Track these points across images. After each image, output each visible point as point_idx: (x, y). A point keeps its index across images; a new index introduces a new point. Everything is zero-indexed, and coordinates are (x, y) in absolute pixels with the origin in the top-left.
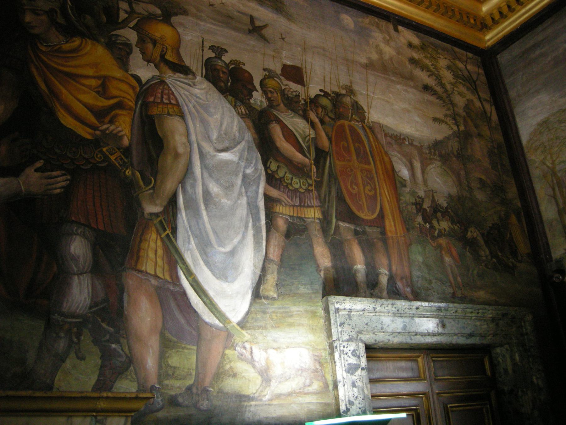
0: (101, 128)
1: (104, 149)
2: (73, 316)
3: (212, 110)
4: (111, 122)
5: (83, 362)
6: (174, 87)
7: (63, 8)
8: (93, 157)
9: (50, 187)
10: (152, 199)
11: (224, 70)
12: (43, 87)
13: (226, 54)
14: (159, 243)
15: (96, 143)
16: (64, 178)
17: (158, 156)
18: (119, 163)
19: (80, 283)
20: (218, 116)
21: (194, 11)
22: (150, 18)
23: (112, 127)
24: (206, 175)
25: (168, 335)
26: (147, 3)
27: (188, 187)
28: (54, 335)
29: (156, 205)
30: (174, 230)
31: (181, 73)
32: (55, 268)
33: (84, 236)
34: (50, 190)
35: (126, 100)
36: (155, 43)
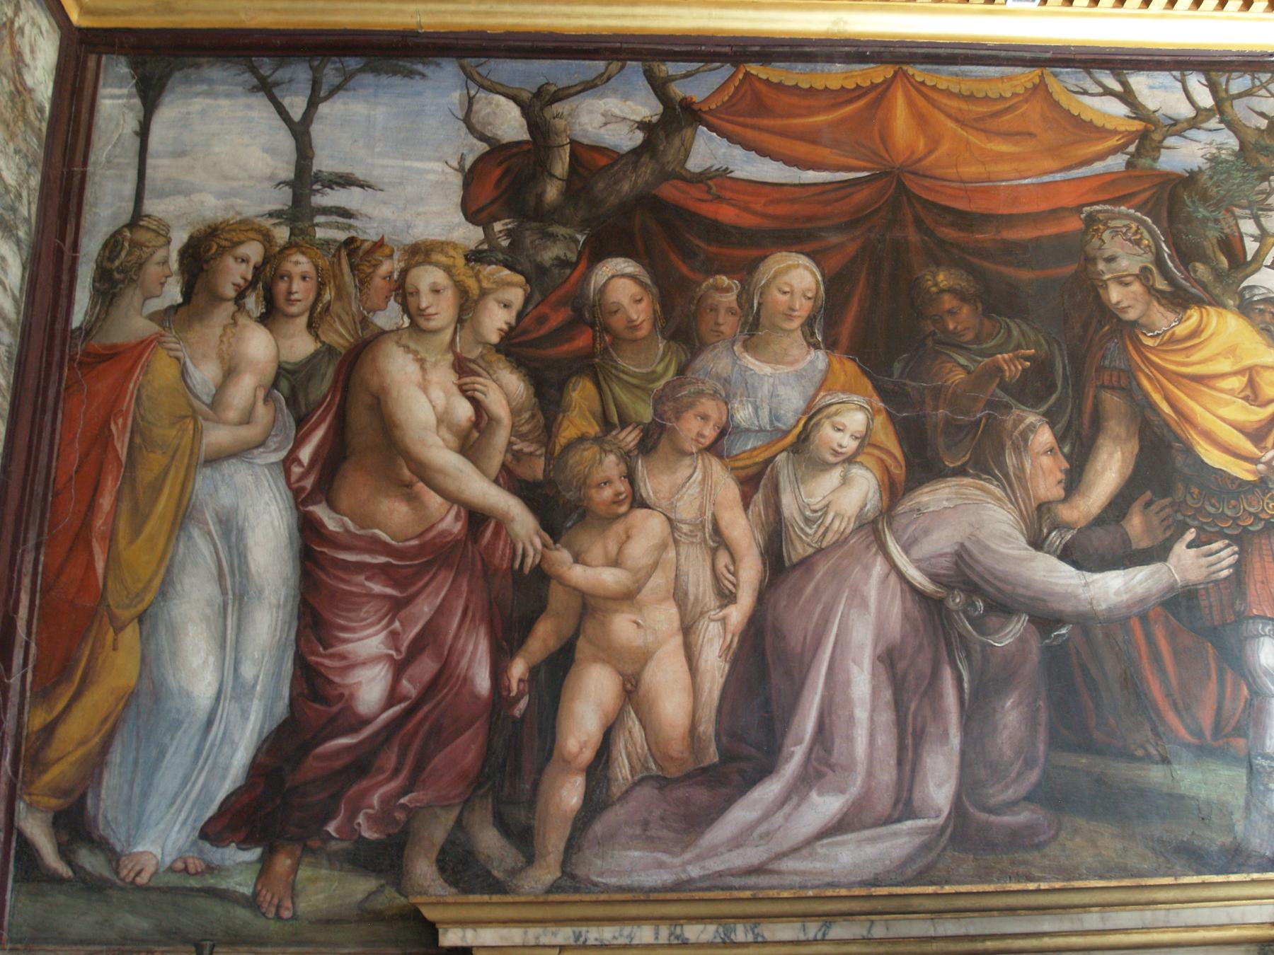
0: (1264, 459)
8: (1263, 509)
16: (1229, 550)
28: (1262, 788)
32: (1245, 691)
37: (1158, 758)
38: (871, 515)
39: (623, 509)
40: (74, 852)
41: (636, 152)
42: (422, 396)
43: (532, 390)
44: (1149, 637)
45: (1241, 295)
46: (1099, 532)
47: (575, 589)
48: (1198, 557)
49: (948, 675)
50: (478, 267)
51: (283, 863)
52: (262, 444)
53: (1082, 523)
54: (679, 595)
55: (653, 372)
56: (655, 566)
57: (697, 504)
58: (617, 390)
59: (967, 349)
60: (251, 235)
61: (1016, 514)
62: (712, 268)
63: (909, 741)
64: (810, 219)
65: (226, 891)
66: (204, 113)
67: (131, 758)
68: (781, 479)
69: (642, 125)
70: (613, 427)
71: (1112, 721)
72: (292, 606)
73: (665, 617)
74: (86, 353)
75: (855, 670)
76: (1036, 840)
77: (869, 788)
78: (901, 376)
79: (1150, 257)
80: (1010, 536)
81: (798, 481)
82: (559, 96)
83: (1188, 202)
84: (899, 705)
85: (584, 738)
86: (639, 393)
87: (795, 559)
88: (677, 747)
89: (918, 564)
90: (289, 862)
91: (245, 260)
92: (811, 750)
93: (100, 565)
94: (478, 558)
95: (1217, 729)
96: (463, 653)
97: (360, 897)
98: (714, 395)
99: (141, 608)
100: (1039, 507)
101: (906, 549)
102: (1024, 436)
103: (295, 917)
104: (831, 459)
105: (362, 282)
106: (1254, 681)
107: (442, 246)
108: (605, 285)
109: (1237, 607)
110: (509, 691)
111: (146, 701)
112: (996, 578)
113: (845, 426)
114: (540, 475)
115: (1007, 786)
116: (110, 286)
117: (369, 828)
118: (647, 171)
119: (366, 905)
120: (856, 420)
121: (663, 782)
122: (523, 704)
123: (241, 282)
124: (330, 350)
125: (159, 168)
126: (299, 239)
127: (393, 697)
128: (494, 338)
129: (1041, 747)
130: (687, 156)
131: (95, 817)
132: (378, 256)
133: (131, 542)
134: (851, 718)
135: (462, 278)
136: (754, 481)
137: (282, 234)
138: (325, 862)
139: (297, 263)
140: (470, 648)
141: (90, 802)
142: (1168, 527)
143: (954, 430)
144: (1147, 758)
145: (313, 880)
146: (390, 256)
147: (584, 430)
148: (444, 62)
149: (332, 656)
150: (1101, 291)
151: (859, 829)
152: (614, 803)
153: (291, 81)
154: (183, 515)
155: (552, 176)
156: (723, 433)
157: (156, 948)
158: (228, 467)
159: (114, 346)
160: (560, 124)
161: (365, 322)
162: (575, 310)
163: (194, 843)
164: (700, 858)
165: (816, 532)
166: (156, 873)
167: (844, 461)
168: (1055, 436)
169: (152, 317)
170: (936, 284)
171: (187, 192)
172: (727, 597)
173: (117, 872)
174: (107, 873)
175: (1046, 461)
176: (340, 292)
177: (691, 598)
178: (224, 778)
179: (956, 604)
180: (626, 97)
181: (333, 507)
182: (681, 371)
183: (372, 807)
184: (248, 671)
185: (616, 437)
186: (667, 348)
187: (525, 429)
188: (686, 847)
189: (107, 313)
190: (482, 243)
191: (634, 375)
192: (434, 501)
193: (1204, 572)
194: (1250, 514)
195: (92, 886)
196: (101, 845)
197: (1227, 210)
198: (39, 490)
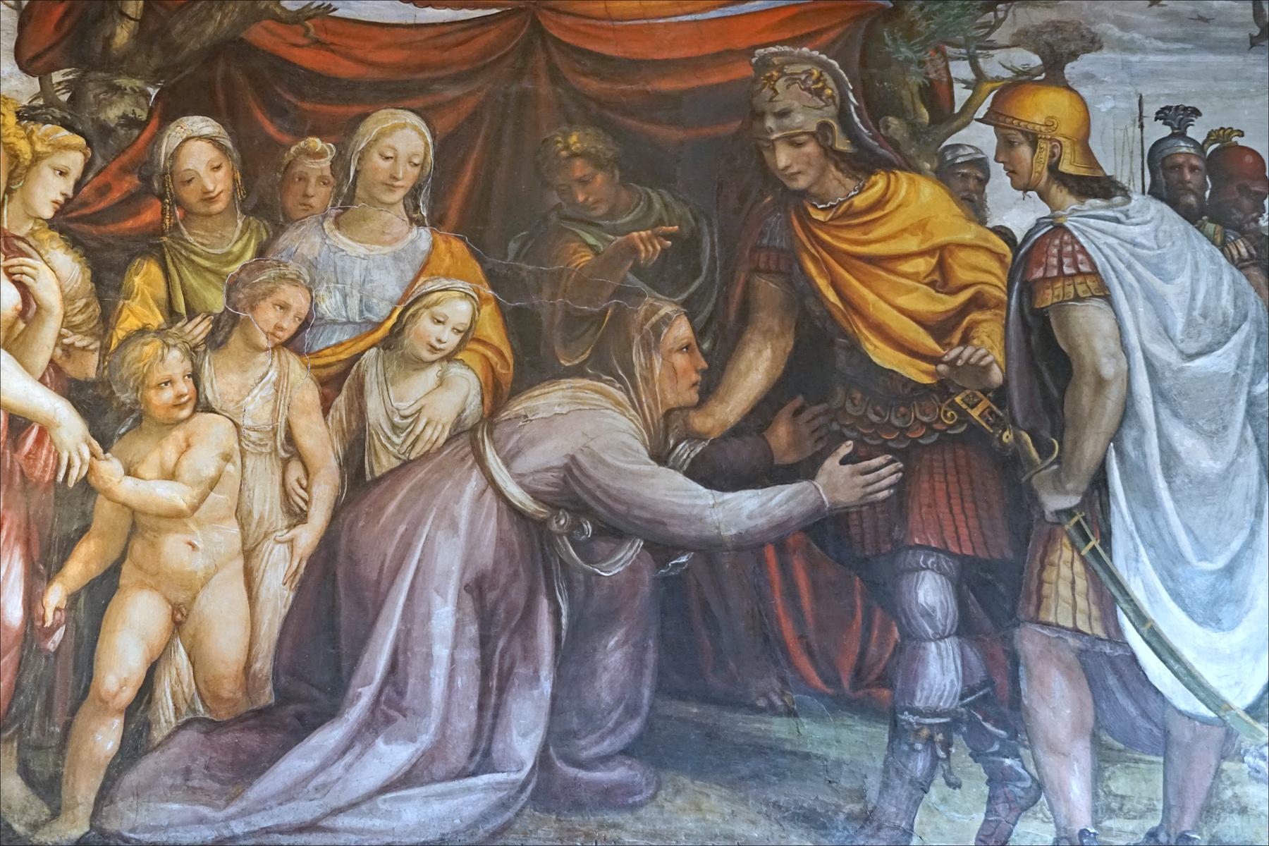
0: (946, 358)
1: (958, 399)
2: (935, 714)
3: (1171, 267)
4: (965, 341)
5: (958, 791)
6: (1083, 233)
7: (843, 115)
8: (939, 418)
9: (870, 489)
10: (1058, 484)
11: (1195, 162)
12: (831, 296)
13: (1197, 121)
14: (1078, 567)
15: (943, 389)
16: (892, 467)
17: (1063, 392)
18: (987, 422)
19: (940, 654)
20: (1185, 279)
21: (1116, 32)
22: (1020, 82)
23: (968, 352)
24: (1165, 413)
25: (1106, 738)
26: (1008, 47)
27: (1129, 446)
28: (906, 748)
29: (1067, 493)
30: (1106, 539)
31: (1096, 196)
32: (896, 634)
33: (939, 570)
34: (871, 494)
35: (987, 288)
36: (1033, 140)
37: (782, 709)
38: (469, 423)
39: (186, 413)
43: (89, 273)
44: (785, 569)
45: (942, 155)
46: (736, 443)
47: (124, 505)
48: (853, 475)
49: (544, 605)
50: (32, 126)
53: (715, 434)
54: (241, 515)
55: (229, 253)
59: (599, 225)
61: (640, 423)
63: (494, 683)
64: (422, 67)
68: (367, 378)
70: (180, 317)
71: (732, 665)
75: (437, 600)
76: (630, 801)
77: (444, 735)
78: (515, 259)
79: (832, 109)
80: (629, 447)
81: (387, 382)
83: (888, 41)
84: (485, 642)
87: (378, 474)
88: (228, 689)
89: (519, 479)
92: (381, 691)
95: (859, 674)
100: (669, 413)
101: (508, 462)
102: (657, 331)
104: (427, 355)
106: (909, 623)
109: (895, 534)
112: (610, 496)
113: (446, 317)
114: (92, 374)
115: (602, 738)
120: (460, 311)
121: (212, 727)
122: (58, 636)
128: (48, 213)
129: (646, 693)
134: (428, 658)
136: (336, 382)
142: (821, 438)
143: (574, 323)
144: (772, 710)
150: (766, 154)
151: (428, 783)
155: (123, 15)
156: (305, 324)
162: (141, 178)
164: (245, 813)
165: (404, 442)
167: (442, 359)
168: (694, 329)
170: (567, 147)
172: (298, 516)
175: (680, 360)
177: (256, 516)
179: (562, 527)
182: (261, 252)
186: (247, 226)
187: (78, 319)
188: (231, 800)
190: (36, 97)
191: (207, 257)
193: (858, 492)
194: (923, 423)
197: (937, 50)
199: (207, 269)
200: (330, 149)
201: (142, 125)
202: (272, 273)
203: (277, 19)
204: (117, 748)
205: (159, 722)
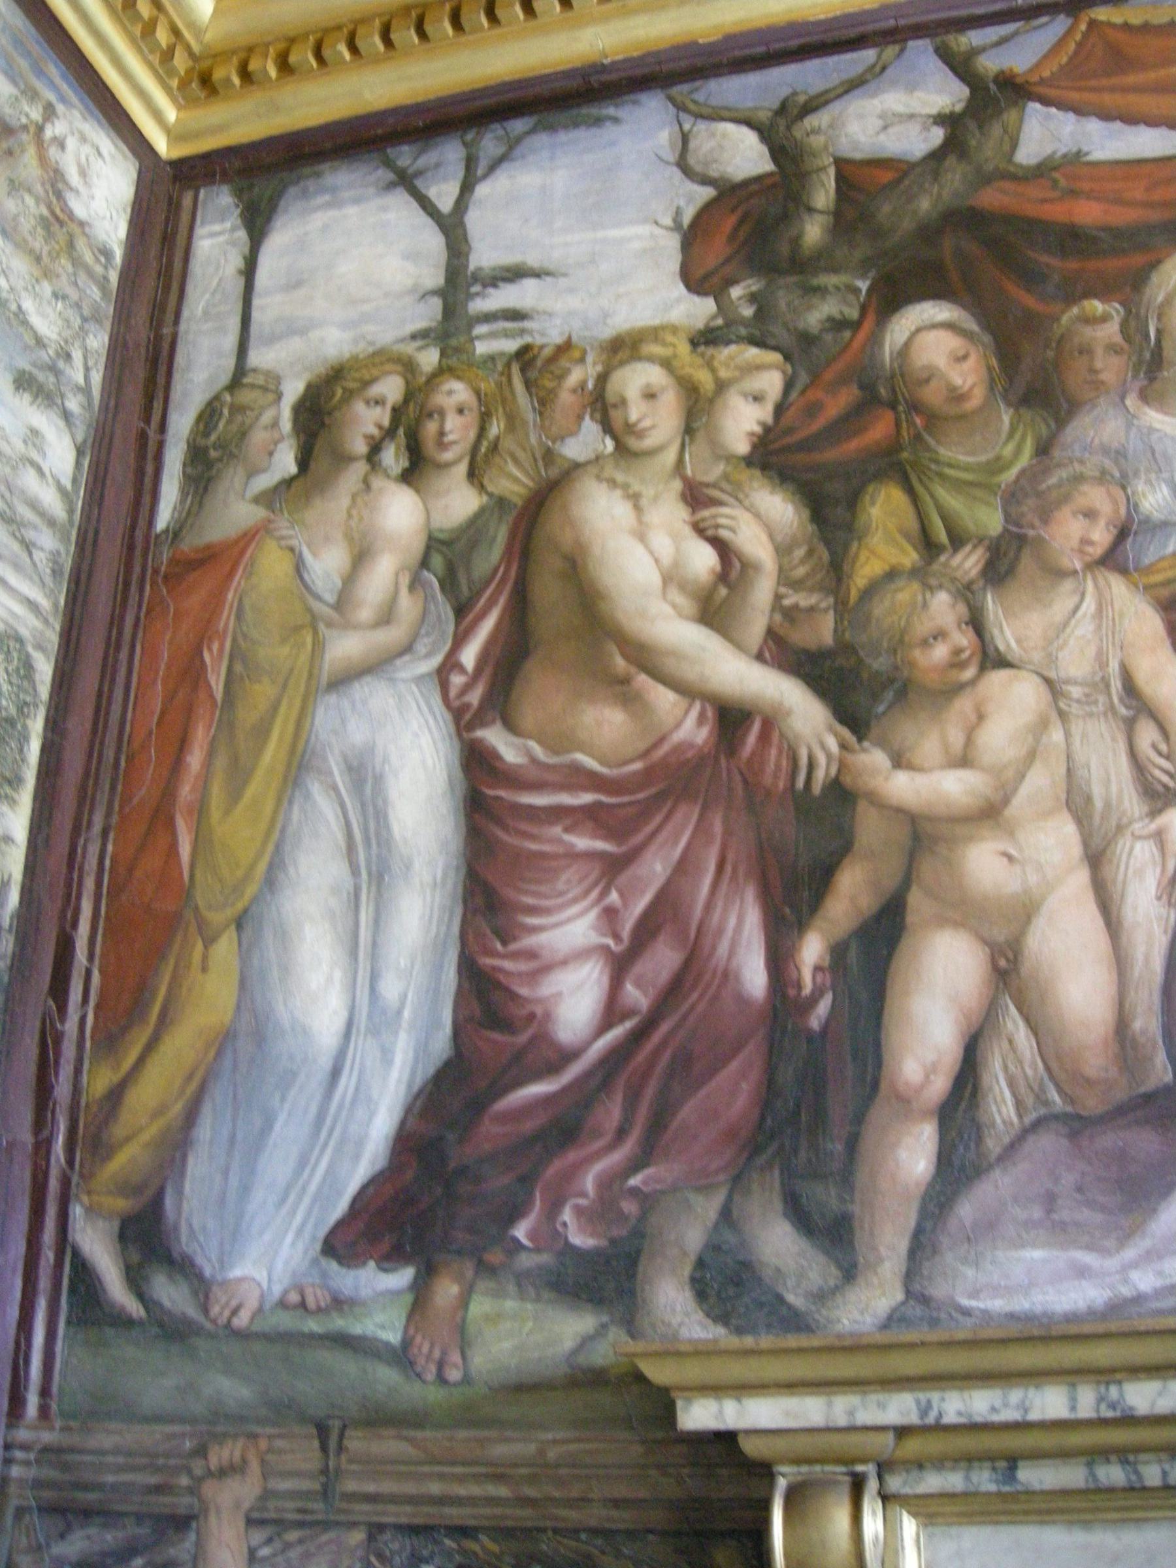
39: (969, 673)
40: (146, 1279)
41: (936, 156)
42: (638, 547)
43: (806, 514)
47: (899, 810)
50: (710, 351)
51: (447, 1290)
52: (407, 649)
54: (1076, 802)
55: (998, 458)
56: (1031, 756)
57: (1091, 651)
58: (941, 493)
60: (389, 367)
62: (1073, 292)
65: (362, 1339)
66: (325, 228)
67: (225, 1133)
69: (940, 119)
72: (454, 882)
73: (1054, 843)
74: (173, 561)
82: (811, 106)
85: (931, 1057)
86: (978, 493)
88: (1096, 1062)
90: (455, 1289)
91: (379, 402)
93: (185, 850)
94: (738, 778)
96: (720, 931)
97: (568, 1344)
98: (1103, 478)
99: (240, 906)
103: (467, 1380)
105: (543, 402)
107: (654, 334)
108: (907, 344)
110: (799, 986)
111: (245, 1043)
116: (203, 469)
117: (581, 1230)
118: (955, 177)
119: (581, 1360)
121: (1076, 1125)
122: (823, 1007)
123: (375, 432)
124: (501, 503)
125: (266, 309)
126: (453, 362)
127: (611, 1012)
128: (742, 447)
130: (1014, 145)
131: (176, 1228)
132: (564, 362)
133: (227, 812)
135: (688, 370)
137: (429, 359)
138: (511, 1288)
139: (450, 393)
140: (732, 922)
141: (169, 1202)
145: (494, 1319)
146: (582, 360)
147: (894, 561)
148: (644, 97)
149: (515, 956)
152: (990, 1167)
153: (438, 165)
154: (299, 766)
155: (811, 210)
157: (258, 1430)
158: (360, 690)
159: (208, 547)
160: (817, 141)
161: (549, 456)
162: (862, 387)
163: (315, 1262)
164: (1151, 1256)
166: (260, 1310)
169: (257, 500)
171: (303, 332)
173: (206, 1310)
174: (192, 1312)
176: (513, 421)
177: (1098, 804)
178: (357, 1157)
180: (911, 87)
181: (511, 726)
182: (1043, 450)
183: (583, 1194)
184: (391, 988)
185: (946, 565)
187: (801, 571)
188: (1126, 1237)
189: (201, 504)
190: (714, 318)
191: (966, 468)
192: (664, 699)
195: (173, 1332)
196: (183, 1267)
198: (109, 753)
199: (971, 484)
200: (1115, 310)
201: (856, 326)
202: (1064, 474)
203: (1015, 178)
204: (932, 1169)
205: (993, 1124)
